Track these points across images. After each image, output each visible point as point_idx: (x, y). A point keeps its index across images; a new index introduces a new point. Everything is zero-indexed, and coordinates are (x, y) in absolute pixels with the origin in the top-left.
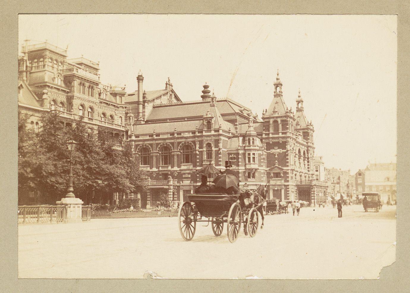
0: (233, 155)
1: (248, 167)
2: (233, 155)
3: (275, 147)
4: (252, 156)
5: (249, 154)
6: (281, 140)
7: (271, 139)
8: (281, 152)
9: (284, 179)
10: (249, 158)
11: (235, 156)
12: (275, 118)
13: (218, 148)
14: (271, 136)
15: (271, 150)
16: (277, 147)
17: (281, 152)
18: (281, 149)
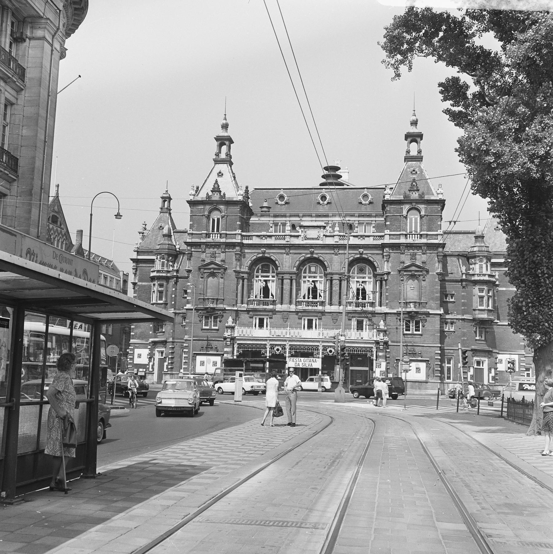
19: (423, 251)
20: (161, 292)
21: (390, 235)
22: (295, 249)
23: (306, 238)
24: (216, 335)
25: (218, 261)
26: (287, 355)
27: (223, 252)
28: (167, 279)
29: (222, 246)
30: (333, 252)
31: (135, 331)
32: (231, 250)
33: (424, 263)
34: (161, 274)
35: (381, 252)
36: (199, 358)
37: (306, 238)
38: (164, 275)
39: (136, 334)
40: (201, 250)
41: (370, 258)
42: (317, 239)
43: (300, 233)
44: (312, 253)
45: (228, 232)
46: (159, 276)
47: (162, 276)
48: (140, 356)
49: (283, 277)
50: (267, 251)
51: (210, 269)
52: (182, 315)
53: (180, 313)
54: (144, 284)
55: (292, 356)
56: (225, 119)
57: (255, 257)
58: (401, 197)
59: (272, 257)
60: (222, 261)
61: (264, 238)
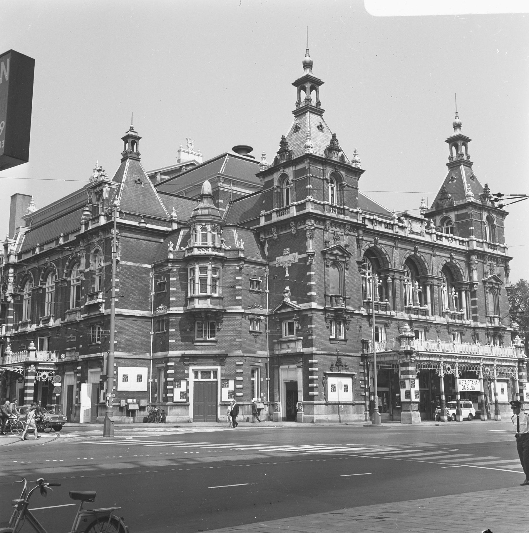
9: (302, 338)
12: (282, 170)
14: (275, 218)
15: (277, 258)
16: (288, 249)
17: (297, 261)
19: (497, 263)
20: (214, 280)
21: (477, 241)
22: (402, 243)
23: (412, 232)
24: (344, 347)
25: (342, 244)
26: (458, 375)
27: (347, 235)
28: (222, 260)
29: (347, 226)
30: (431, 252)
31: (119, 338)
32: (352, 233)
33: (499, 275)
34: (218, 254)
35: (464, 259)
36: (331, 381)
37: (412, 232)
38: (222, 254)
39: (119, 342)
40: (323, 227)
41: (457, 264)
42: (420, 234)
43: (406, 223)
44: (416, 250)
45: (351, 210)
46: (216, 255)
47: (220, 256)
48: (139, 378)
49: (393, 276)
50: (380, 241)
51: (335, 255)
52: (250, 316)
53: (248, 314)
54: (129, 263)
55: (462, 377)
56: (308, 55)
57: (368, 247)
58: (479, 202)
59: (383, 250)
60: (346, 246)
61: (375, 224)
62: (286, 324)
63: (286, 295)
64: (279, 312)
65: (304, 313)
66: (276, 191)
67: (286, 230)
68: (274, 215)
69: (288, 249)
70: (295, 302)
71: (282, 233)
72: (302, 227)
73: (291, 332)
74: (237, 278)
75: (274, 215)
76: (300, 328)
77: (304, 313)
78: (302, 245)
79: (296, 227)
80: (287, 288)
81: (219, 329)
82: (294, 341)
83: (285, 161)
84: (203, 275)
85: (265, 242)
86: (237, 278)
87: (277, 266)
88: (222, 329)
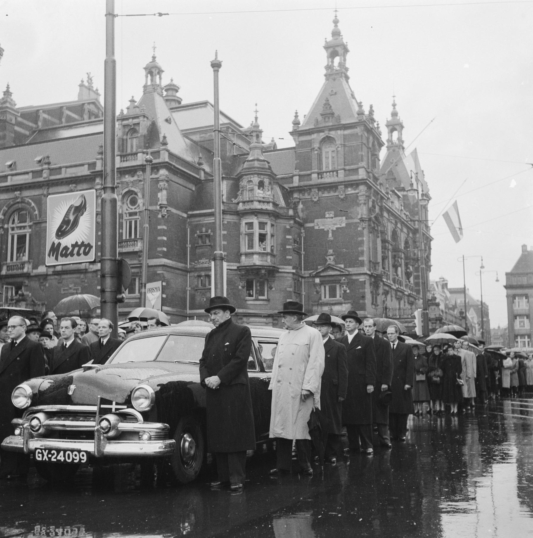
0: (204, 230)
1: (245, 261)
2: (204, 230)
3: (326, 213)
4: (257, 231)
5: (250, 225)
6: (340, 193)
7: (316, 190)
8: (344, 225)
10: (250, 236)
11: (210, 231)
12: (327, 132)
13: (156, 204)
15: (316, 221)
18: (344, 218)
62: (325, 287)
63: (332, 258)
64: (322, 274)
65: (354, 277)
66: (316, 152)
67: (329, 193)
68: (314, 176)
69: (333, 212)
70: (342, 266)
71: (324, 195)
72: (353, 192)
73: (333, 294)
74: (288, 237)
75: (314, 176)
76: (348, 291)
77: (354, 277)
78: (352, 210)
79: (344, 191)
80: (331, 251)
81: (271, 288)
82: (340, 304)
83: (331, 124)
84: (262, 232)
85: (299, 202)
86: (288, 237)
87: (317, 228)
88: (274, 289)
